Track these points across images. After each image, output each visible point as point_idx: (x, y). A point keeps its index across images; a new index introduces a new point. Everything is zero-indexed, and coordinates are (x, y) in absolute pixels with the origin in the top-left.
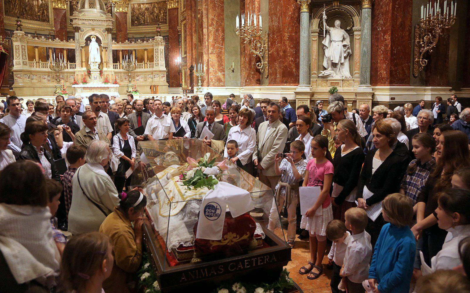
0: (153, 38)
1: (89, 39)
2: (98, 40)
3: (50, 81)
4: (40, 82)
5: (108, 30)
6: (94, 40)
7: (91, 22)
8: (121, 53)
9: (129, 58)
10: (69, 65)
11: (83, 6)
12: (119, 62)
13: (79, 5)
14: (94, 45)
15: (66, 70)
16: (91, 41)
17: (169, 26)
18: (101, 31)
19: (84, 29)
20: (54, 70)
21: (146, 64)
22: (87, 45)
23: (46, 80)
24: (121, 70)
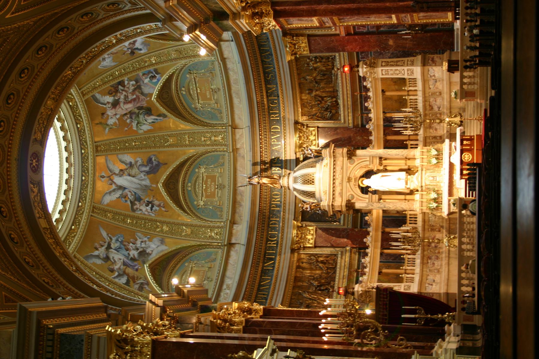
0: (364, 79)
1: (365, 190)
2: (368, 174)
3: (437, 257)
5: (351, 155)
6: (366, 182)
7: (337, 182)
8: (389, 138)
11: (311, 195)
12: (406, 141)
13: (311, 200)
14: (374, 183)
15: (420, 229)
16: (368, 187)
17: (339, 51)
18: (352, 166)
21: (410, 93)
23: (436, 262)
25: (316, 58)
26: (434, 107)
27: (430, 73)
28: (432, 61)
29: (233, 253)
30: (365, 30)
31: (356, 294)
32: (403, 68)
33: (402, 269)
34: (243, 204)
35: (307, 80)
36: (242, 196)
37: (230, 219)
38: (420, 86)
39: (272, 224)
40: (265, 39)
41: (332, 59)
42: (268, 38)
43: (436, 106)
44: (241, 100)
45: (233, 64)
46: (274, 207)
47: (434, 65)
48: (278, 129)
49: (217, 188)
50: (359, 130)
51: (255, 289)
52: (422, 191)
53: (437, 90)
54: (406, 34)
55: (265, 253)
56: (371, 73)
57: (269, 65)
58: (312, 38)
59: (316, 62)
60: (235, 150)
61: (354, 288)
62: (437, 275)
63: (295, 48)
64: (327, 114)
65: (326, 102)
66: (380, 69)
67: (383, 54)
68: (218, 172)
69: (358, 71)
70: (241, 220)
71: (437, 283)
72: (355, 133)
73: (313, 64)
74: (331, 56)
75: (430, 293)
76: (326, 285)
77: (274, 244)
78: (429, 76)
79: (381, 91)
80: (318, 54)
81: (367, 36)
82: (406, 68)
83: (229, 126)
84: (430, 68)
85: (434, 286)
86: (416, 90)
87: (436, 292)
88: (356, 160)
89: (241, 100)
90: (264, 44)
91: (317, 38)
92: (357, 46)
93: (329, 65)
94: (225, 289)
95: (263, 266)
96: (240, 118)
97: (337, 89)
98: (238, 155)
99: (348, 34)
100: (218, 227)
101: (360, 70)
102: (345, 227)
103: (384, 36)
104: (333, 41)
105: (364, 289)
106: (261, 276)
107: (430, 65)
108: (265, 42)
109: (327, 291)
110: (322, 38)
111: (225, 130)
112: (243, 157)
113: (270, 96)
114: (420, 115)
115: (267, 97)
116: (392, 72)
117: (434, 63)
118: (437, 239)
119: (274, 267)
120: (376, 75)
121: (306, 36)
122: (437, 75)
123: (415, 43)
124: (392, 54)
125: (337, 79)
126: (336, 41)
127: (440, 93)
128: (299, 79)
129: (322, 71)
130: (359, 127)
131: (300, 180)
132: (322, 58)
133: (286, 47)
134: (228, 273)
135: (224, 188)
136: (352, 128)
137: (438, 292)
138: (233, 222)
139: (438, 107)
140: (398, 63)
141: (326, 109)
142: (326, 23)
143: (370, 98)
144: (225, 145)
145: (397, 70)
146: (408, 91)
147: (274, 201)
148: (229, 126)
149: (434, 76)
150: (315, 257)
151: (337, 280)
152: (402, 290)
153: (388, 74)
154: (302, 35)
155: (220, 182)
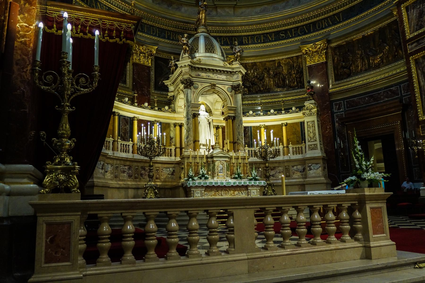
3: (131, 176)
33: (118, 139)
43: (274, 173)
44: (258, 13)
46: (168, 33)
53: (291, 173)
71: (104, 175)
78: (310, 165)
85: (101, 171)
89: (258, 13)
103: (331, 126)
113: (264, 36)
122: (311, 172)
137: (95, 175)
139: (273, 175)
147: (173, 34)
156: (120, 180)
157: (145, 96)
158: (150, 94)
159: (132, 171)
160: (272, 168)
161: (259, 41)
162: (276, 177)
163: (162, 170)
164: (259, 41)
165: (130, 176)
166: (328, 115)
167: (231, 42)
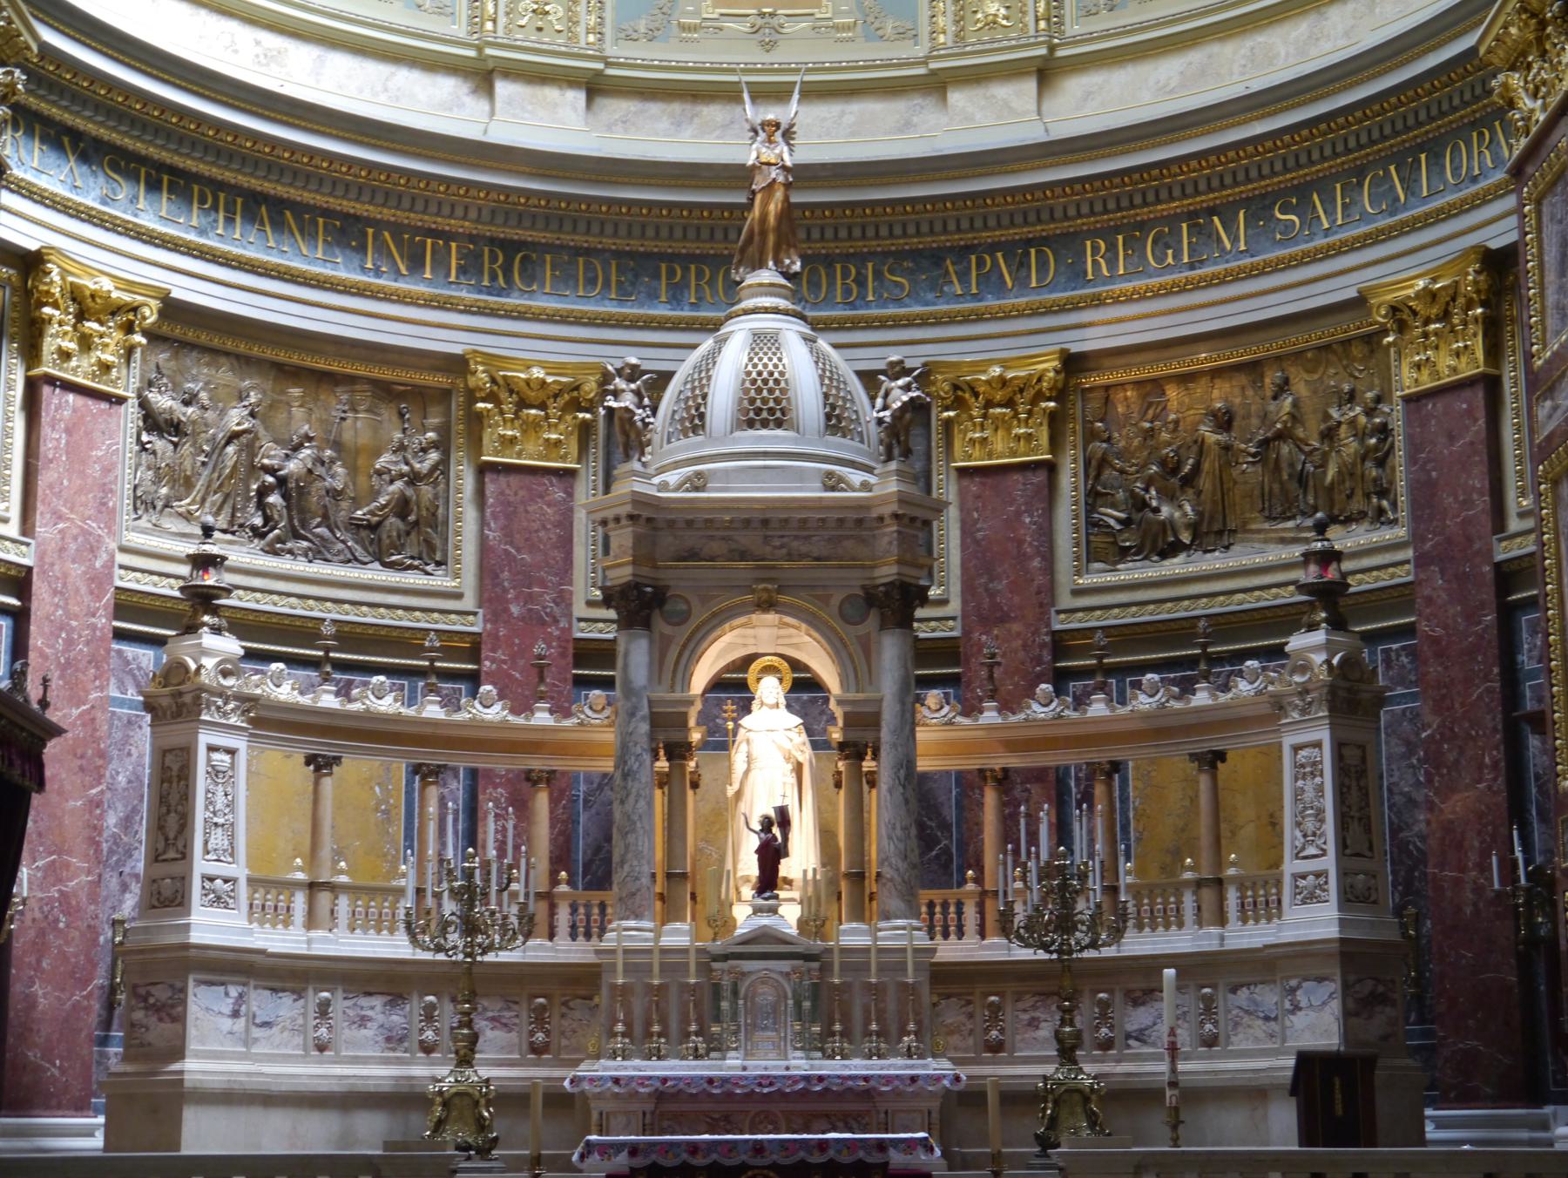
3: (401, 1040)
4: (321, 1048)
6: (770, 690)
8: (990, 798)
9: (1062, 833)
10: (563, 916)
11: (695, 421)
12: (979, 880)
17: (1416, 538)
19: (695, 602)
20: (439, 949)
21: (1208, 894)
22: (721, 743)
23: (368, 1033)
24: (997, 950)
25: (1384, 431)
26: (1142, 1009)
27: (1305, 984)
28: (1372, 993)
29: (447, 87)
30: (1527, 660)
31: (189, 641)
32: (1331, 848)
34: (687, 134)
35: (1275, 398)
36: (725, 127)
37: (610, 72)
38: (1246, 936)
39: (589, 267)
40: (1470, 168)
41: (1381, 511)
42: (1474, 180)
45: (1347, 34)
46: (671, 273)
47: (1351, 1005)
48: (1038, 281)
49: (762, 15)
50: (1039, 662)
51: (255, 184)
52: (708, 960)
54: (1509, 867)
55: (448, 236)
56: (1304, 691)
57: (1344, 205)
58: (1479, 396)
59: (1361, 435)
60: (936, 85)
61: (217, 630)
62: (299, 1040)
63: (1427, 322)
64: (1114, 506)
65: (1169, 496)
66: (1324, 735)
67: (1405, 757)
68: (837, 13)
69: (1312, 627)
70: (609, 128)
71: (248, 1041)
72: (1025, 646)
73: (1353, 422)
74: (1394, 505)
75: (183, 1002)
76: (290, 519)
77: (493, 278)
78: (1293, 983)
79: (1218, 746)
80: (1399, 440)
81: (1496, 670)
82: (1329, 863)
83: (1052, 48)
84: (1333, 986)
85: (227, 1024)
86: (1222, 920)
87: (192, 1032)
88: (861, 629)
89: (1171, 92)
90: (1444, 167)
91: (1482, 422)
92: (1445, 627)
93: (1349, 497)
94: (258, 43)
95: (378, 224)
96: (1088, 95)
97: (1236, 548)
98: (917, 101)
99: (1509, 576)
100: (573, 21)
101: (1319, 637)
102: (580, 610)
103: (1498, 754)
104: (1467, 503)
105: (205, 678)
106: (327, 213)
107: (1346, 987)
108: (1456, 171)
109: (258, 521)
110: (1482, 448)
111: (1032, 32)
112: (907, 125)
114: (1094, 945)
115: (1191, 216)
116: (1309, 794)
117: (1356, 1008)
118: (474, 1039)
119: (378, 272)
120: (1296, 715)
121: (1491, 371)
122: (1299, 1020)
123: (1468, 910)
124: (1411, 802)
125: (1283, 541)
126: (1467, 522)
127: (1211, 1042)
128: (1278, 359)
129: (1323, 465)
130: (1056, 659)
131: (767, 363)
132: (1381, 463)
133: (1434, 280)
134: (341, 64)
135: (762, 44)
136: (1048, 625)
137: (192, 1045)
138: (596, 87)
139: (1141, 1031)
140: (1355, 827)
141: (1142, 505)
142: (1548, 404)
143: (1178, 698)
144: (959, 36)
145: (1322, 821)
146: (1219, 883)
148: (1052, 48)
149: (1296, 1008)
150: (434, 468)
151: (318, 569)
152: (201, 865)
153: (1301, 772)
154: (1494, 351)
155: (790, 28)
156: (339, 1060)
157: (543, 623)
158: (570, 615)
159: (405, 1017)
160: (1138, 994)
161: (1170, 260)
162: (1154, 1045)
163: (564, 1009)
164: (1170, 260)
165: (394, 1040)
166: (1488, 690)
167: (1023, 273)
